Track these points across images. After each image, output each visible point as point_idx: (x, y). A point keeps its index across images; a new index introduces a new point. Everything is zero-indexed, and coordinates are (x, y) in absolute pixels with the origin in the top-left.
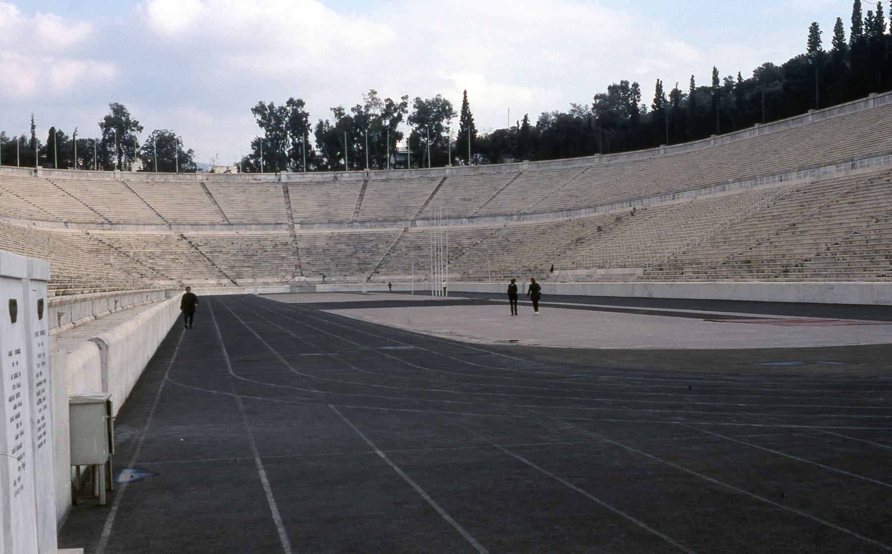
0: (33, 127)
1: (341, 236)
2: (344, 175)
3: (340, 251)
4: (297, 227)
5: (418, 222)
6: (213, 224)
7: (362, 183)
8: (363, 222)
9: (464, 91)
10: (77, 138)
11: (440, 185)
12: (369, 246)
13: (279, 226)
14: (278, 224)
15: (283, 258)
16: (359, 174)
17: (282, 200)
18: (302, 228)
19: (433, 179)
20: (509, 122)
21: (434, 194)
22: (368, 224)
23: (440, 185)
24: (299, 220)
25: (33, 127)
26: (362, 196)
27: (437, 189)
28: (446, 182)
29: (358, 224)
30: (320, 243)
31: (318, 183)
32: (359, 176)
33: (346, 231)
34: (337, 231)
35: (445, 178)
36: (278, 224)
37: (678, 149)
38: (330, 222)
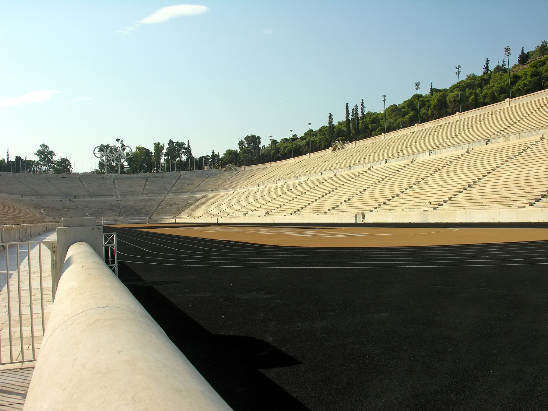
0: (8, 155)
1: (138, 200)
2: (139, 175)
3: (137, 206)
4: (119, 196)
5: (170, 194)
6: (84, 196)
8: (147, 194)
10: (27, 160)
12: (150, 204)
13: (112, 196)
14: (112, 195)
15: (114, 210)
16: (145, 175)
18: (121, 197)
19: (175, 177)
22: (149, 195)
24: (120, 194)
25: (8, 155)
29: (145, 195)
30: (130, 204)
31: (128, 178)
32: (144, 176)
33: (141, 198)
34: (136, 198)
35: (180, 176)
36: (112, 195)
38: (133, 194)
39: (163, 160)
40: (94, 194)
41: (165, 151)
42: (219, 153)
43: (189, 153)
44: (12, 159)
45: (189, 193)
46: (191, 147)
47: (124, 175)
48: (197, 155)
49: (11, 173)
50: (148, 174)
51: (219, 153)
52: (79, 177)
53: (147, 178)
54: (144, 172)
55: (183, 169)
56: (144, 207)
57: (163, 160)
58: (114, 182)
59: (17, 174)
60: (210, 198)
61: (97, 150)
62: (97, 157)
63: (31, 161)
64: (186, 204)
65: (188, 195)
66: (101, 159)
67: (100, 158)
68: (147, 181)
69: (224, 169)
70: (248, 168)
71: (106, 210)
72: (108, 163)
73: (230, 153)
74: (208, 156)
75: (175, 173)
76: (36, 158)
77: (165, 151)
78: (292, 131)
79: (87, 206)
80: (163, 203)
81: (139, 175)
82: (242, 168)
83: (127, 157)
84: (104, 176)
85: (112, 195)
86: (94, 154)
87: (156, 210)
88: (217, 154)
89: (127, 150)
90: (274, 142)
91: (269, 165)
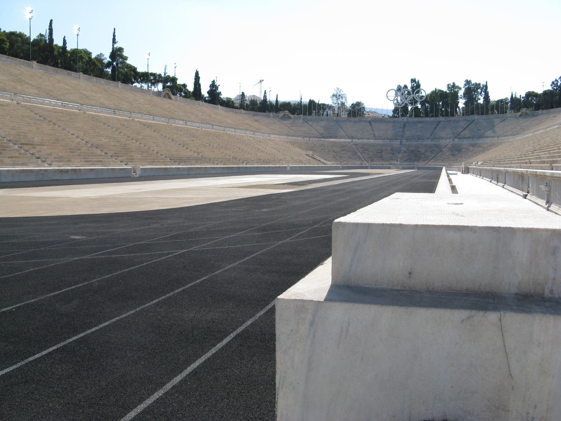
0: (301, 99)
3: (419, 151)
4: (404, 140)
5: (456, 140)
7: (438, 122)
9: (486, 82)
10: (320, 103)
11: (470, 124)
16: (438, 119)
17: (401, 130)
19: (468, 121)
20: (505, 95)
21: (467, 127)
22: (435, 140)
23: (470, 124)
25: (301, 99)
26: (436, 128)
27: (469, 125)
28: (474, 122)
35: (474, 120)
38: (419, 139)
39: (461, 103)
40: (379, 138)
41: (461, 93)
42: (520, 96)
44: (306, 101)
45: (475, 139)
46: (489, 90)
47: (416, 119)
48: (494, 97)
49: (302, 115)
50: (441, 119)
51: (520, 96)
52: (371, 121)
53: (440, 122)
55: (478, 114)
56: (425, 152)
57: (461, 103)
58: (404, 126)
59: (308, 117)
61: (393, 93)
62: (391, 100)
63: (324, 105)
64: (467, 150)
65: (474, 141)
66: (394, 102)
67: (393, 102)
68: (438, 125)
69: (519, 114)
70: (545, 111)
71: (385, 154)
72: (401, 106)
73: (530, 95)
74: (506, 99)
75: (470, 117)
77: (461, 93)
79: (367, 150)
80: (445, 149)
81: (432, 119)
83: (421, 100)
84: (396, 119)
85: (397, 138)
86: (387, 97)
87: (435, 156)
88: (518, 97)
89: (423, 94)
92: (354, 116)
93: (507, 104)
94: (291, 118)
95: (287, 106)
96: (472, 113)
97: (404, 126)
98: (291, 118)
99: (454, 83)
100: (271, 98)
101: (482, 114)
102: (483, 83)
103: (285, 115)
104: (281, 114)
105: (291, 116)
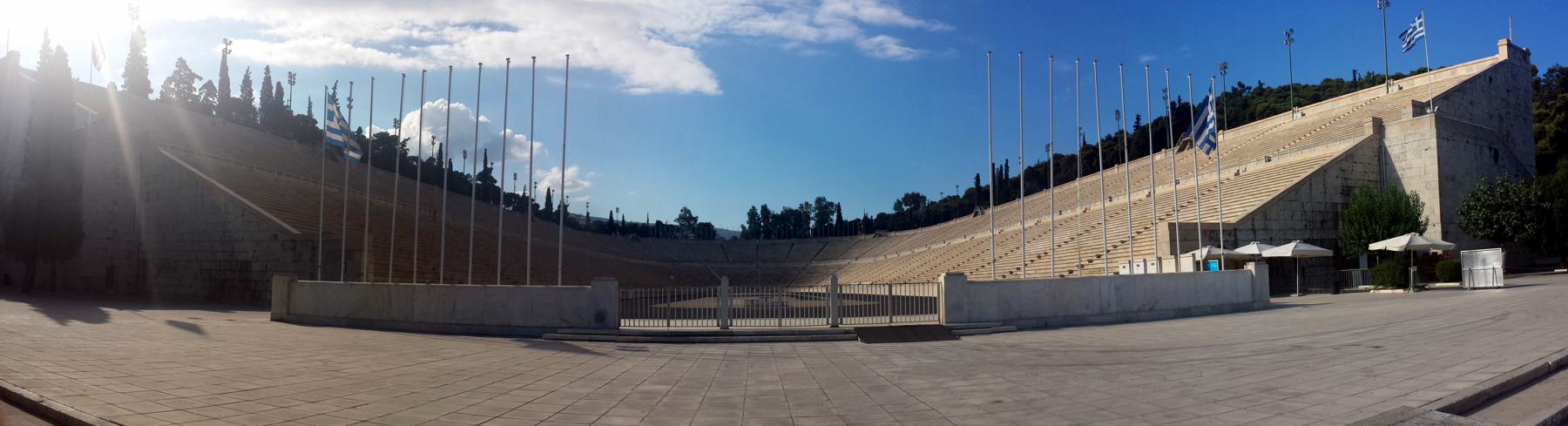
10: (668, 223)
37: (926, 230)
39: (812, 223)
43: (839, 216)
44: (653, 221)
47: (768, 241)
48: (848, 216)
50: (794, 240)
54: (789, 238)
55: (831, 235)
57: (812, 223)
58: (757, 249)
60: (855, 265)
69: (873, 235)
70: (897, 234)
73: (882, 216)
74: (859, 220)
75: (825, 239)
76: (677, 224)
78: (942, 193)
81: (785, 241)
82: (893, 234)
88: (869, 217)
90: (933, 203)
91: (919, 230)
92: (704, 238)
93: (860, 225)
94: (638, 240)
95: (634, 228)
96: (826, 236)
97: (757, 249)
98: (638, 240)
99: (807, 203)
100: (617, 217)
101: (836, 235)
102: (836, 203)
103: (634, 237)
104: (631, 236)
105: (641, 239)
